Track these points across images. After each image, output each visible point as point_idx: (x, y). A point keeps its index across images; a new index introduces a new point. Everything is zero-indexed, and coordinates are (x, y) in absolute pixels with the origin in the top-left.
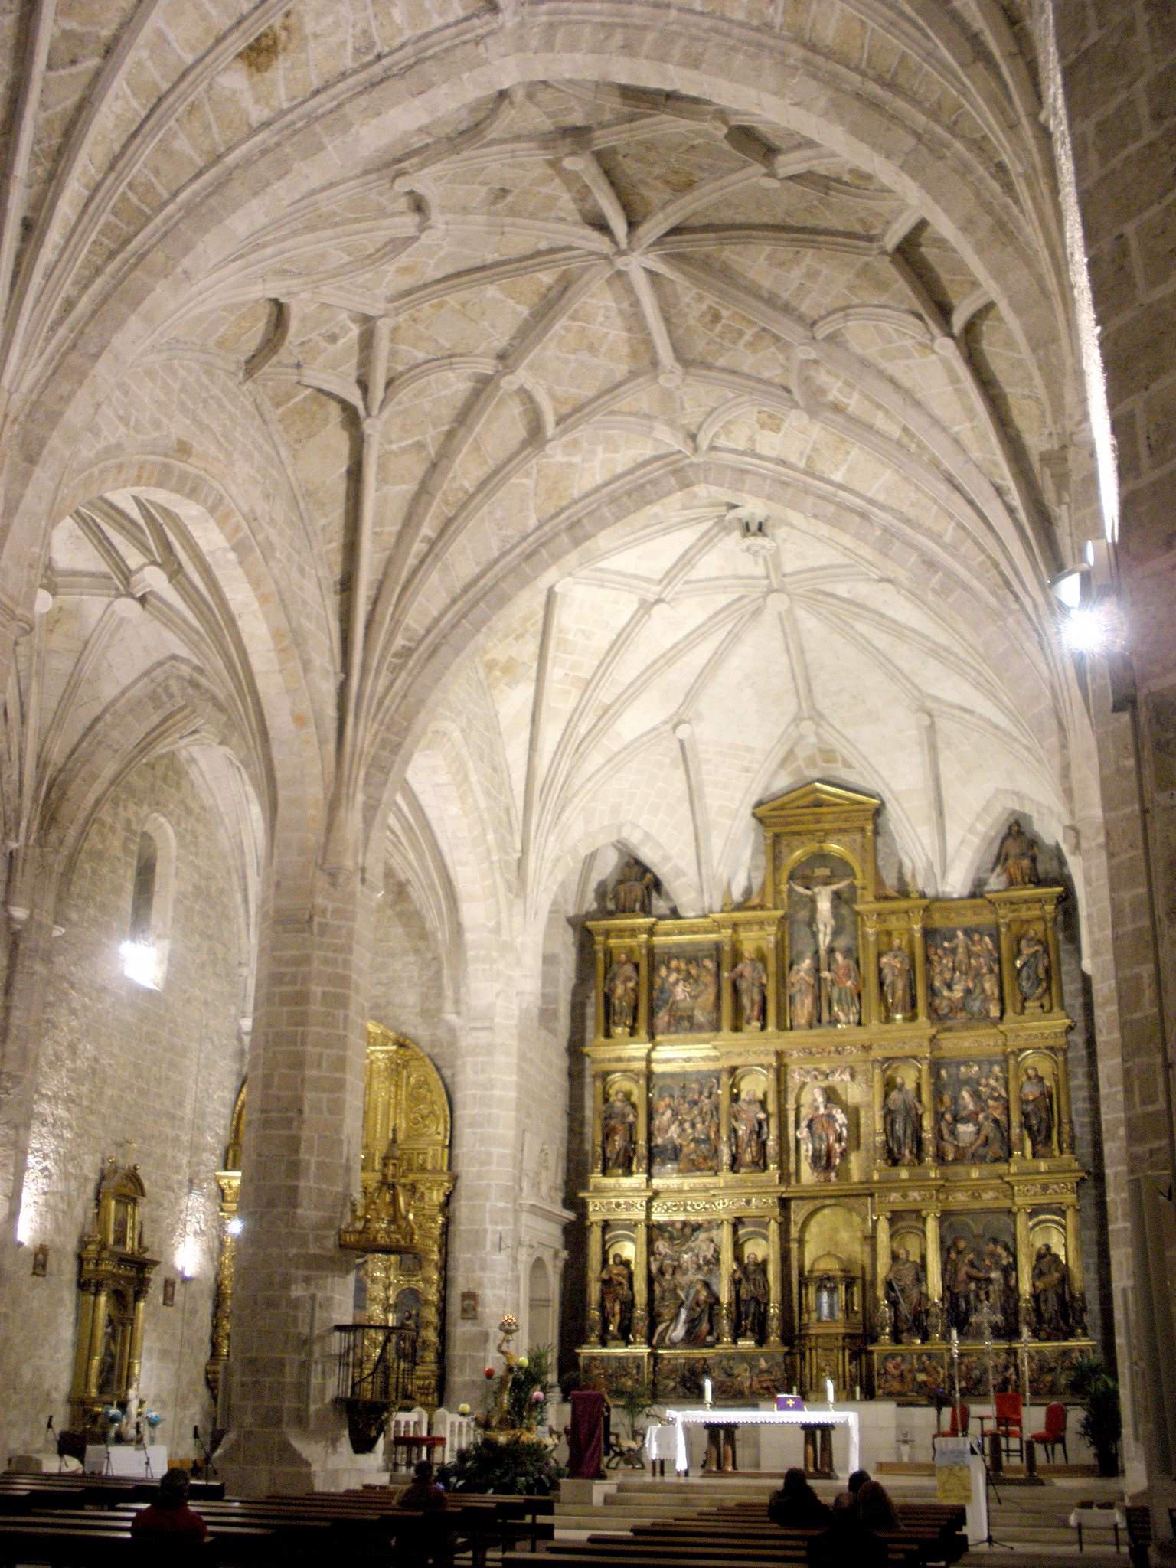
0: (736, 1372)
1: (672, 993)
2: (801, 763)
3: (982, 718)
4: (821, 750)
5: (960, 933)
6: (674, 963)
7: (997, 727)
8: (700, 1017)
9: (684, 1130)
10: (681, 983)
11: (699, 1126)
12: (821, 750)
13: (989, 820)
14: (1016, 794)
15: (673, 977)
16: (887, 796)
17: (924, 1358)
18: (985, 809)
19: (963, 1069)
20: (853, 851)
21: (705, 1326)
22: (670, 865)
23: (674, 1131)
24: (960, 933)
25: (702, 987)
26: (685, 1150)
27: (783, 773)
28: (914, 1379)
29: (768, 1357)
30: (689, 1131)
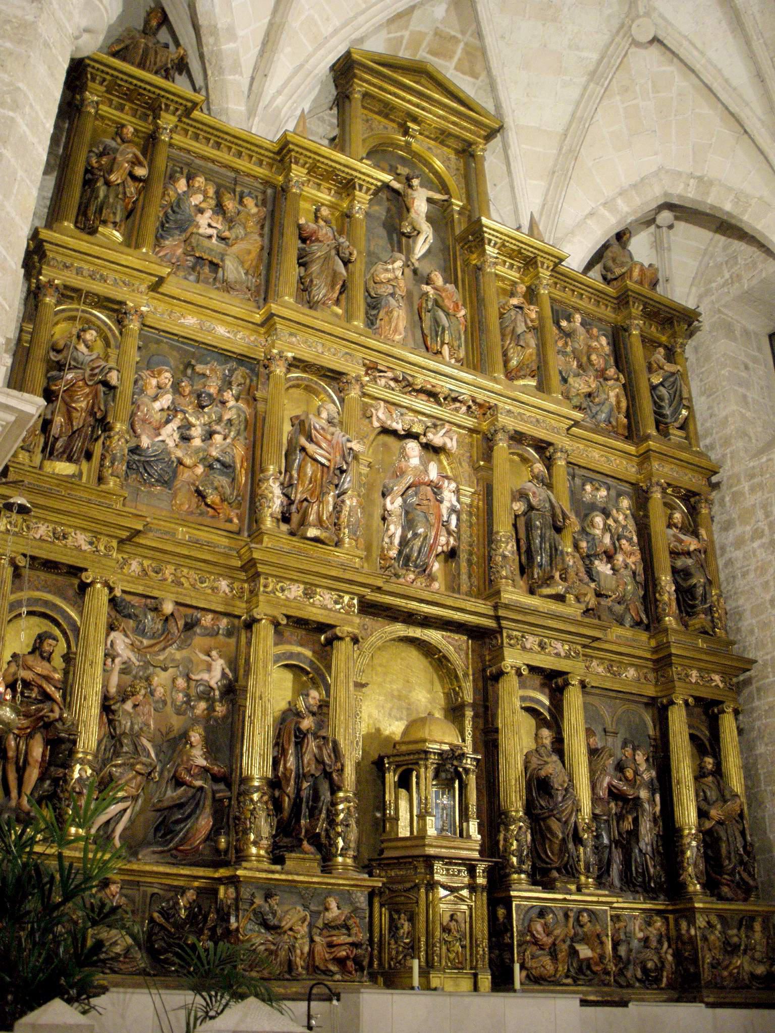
0: (286, 924)
1: (191, 221)
2: (406, 34)
3: (709, 61)
4: (437, 33)
5: (578, 317)
6: (200, 181)
7: (727, 81)
8: (232, 270)
9: (186, 439)
10: (209, 213)
11: (218, 438)
12: (437, 33)
13: (638, 201)
14: (700, 179)
15: (197, 199)
16: (509, 121)
17: (585, 918)
18: (634, 186)
19: (588, 488)
20: (448, 168)
21: (204, 822)
22: (232, 45)
23: (170, 434)
24: (578, 317)
25: (240, 231)
26: (185, 475)
27: (383, 34)
28: (574, 953)
29: (345, 897)
30: (197, 442)
